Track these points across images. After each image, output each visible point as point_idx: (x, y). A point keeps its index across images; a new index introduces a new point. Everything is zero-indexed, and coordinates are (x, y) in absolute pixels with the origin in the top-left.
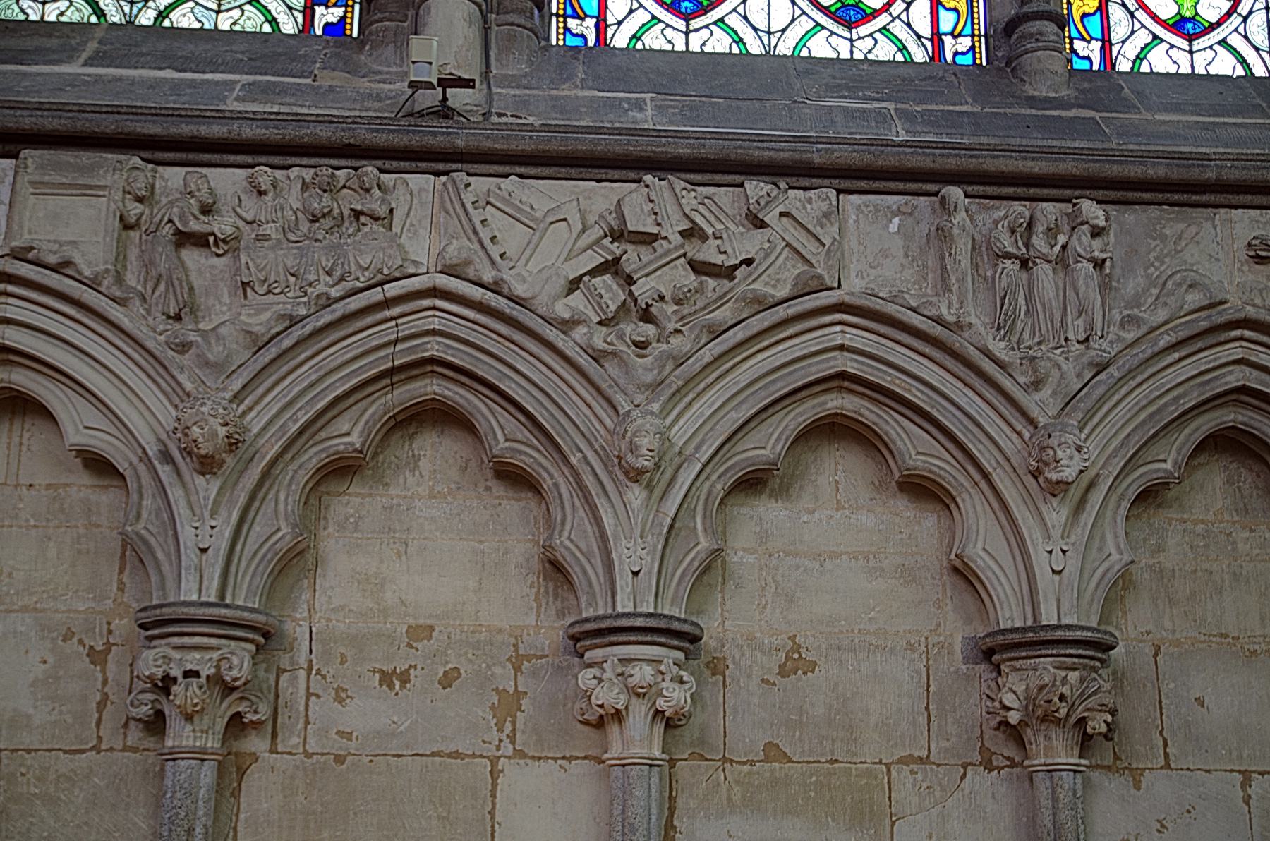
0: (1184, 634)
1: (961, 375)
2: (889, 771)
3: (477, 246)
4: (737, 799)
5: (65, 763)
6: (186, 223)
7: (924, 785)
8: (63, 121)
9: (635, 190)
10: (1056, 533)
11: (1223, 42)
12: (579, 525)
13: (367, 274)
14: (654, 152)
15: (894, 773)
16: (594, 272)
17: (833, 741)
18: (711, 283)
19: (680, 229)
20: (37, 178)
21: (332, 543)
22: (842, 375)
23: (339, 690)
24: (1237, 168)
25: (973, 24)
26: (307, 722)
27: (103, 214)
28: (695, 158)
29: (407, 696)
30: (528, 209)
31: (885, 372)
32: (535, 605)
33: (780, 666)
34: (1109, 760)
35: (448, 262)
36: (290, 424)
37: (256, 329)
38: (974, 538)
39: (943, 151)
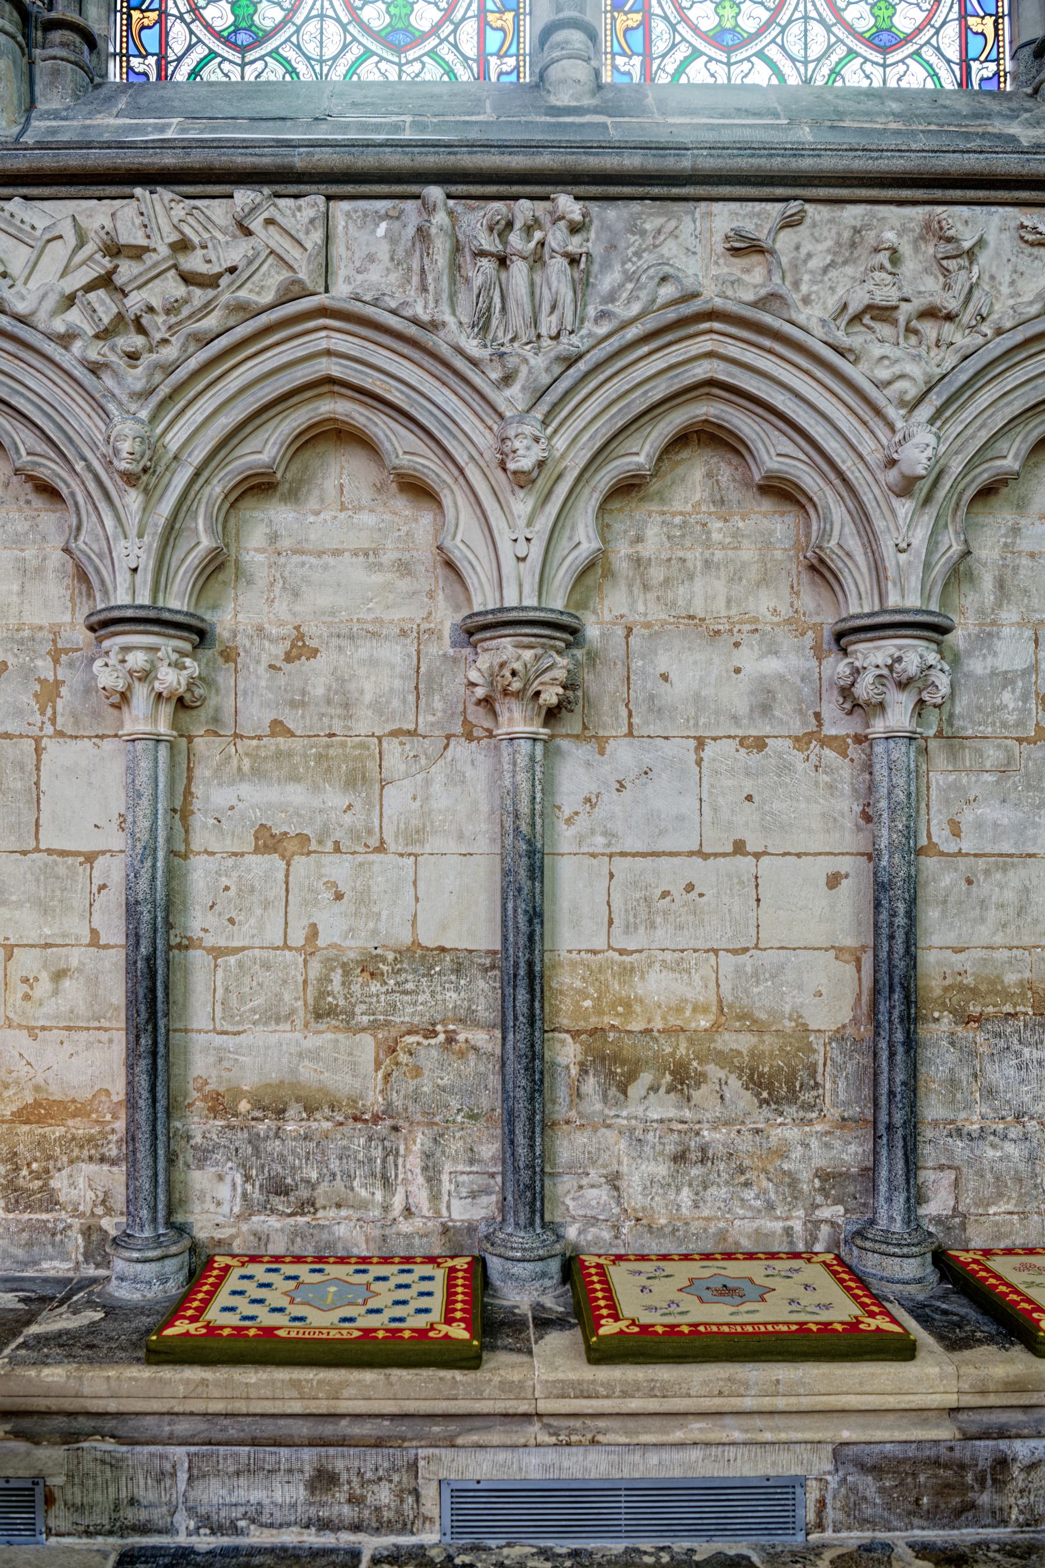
1: (437, 373)
2: (380, 742)
7: (411, 754)
10: (522, 523)
11: (760, 54)
14: (141, 164)
15: (385, 745)
16: (89, 288)
18: (197, 292)
19: (170, 240)
22: (330, 380)
25: (518, 43)
28: (182, 169)
30: (29, 229)
31: (367, 374)
32: (69, 605)
34: (577, 729)
38: (452, 530)
39: (423, 149)
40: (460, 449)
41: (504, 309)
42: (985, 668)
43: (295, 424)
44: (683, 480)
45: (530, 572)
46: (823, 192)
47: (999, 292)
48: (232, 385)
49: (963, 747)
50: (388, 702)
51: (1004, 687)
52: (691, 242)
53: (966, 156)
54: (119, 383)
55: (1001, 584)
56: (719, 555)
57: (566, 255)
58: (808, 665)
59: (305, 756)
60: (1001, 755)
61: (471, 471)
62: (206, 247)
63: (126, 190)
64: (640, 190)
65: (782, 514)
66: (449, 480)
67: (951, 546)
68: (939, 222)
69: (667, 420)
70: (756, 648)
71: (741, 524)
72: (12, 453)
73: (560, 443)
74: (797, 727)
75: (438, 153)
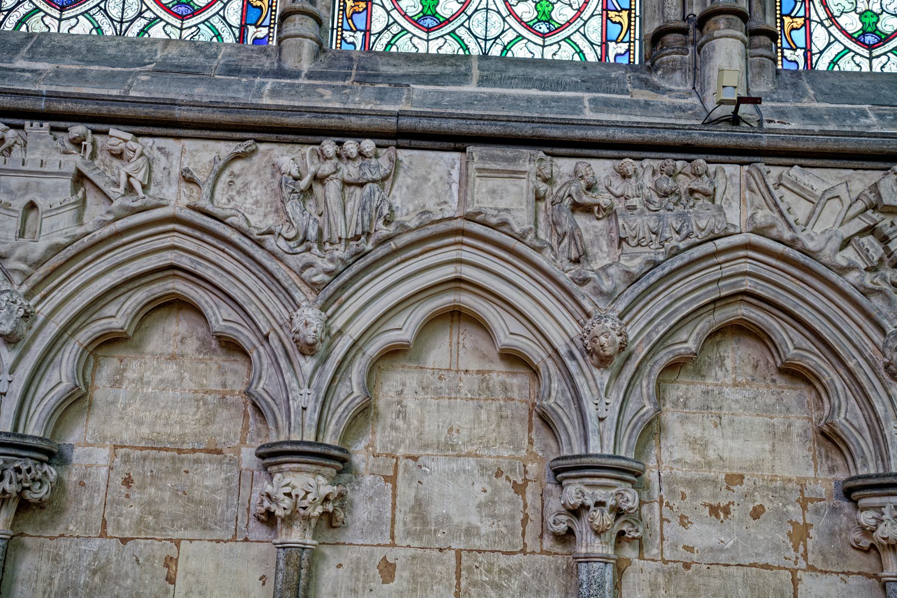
3: (777, 215)
5: (503, 561)
6: (581, 197)
8: (498, 128)
12: (852, 409)
13: (703, 233)
16: (862, 233)
20: (481, 165)
21: (670, 416)
23: (682, 517)
26: (662, 539)
27: (525, 190)
29: (729, 524)
30: (810, 189)
32: (812, 463)
35: (759, 226)
36: (654, 334)
37: (633, 270)
54: (890, 305)
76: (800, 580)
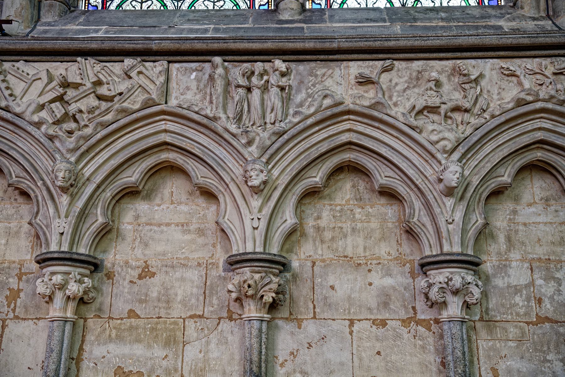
0: (327, 257)
1: (217, 140)
2: (184, 321)
4: (113, 335)
7: (200, 328)
9: (74, 65)
10: (256, 211)
12: (44, 213)
14: (81, 47)
15: (186, 323)
17: (160, 308)
19: (93, 80)
22: (166, 143)
24: (347, 41)
28: (100, 49)
30: (26, 75)
31: (183, 141)
32: (31, 250)
33: (139, 275)
34: (287, 315)
38: (223, 214)
40: (227, 175)
41: (249, 111)
42: (504, 283)
43: (148, 164)
44: (341, 188)
45: (259, 235)
46: (402, 56)
47: (492, 98)
48: (118, 146)
49: (496, 327)
50: (190, 300)
51: (516, 294)
52: (339, 79)
53: (470, 37)
54: (62, 145)
55: (509, 239)
56: (359, 225)
57: (278, 86)
58: (407, 281)
59: (145, 328)
60: (517, 331)
61: (232, 186)
62: (109, 84)
63: (74, 58)
64: (314, 57)
65: (391, 205)
66: (223, 190)
67: (477, 221)
68: (459, 67)
69: (330, 161)
70: (380, 272)
71: (370, 210)
72: (8, 176)
73: (276, 172)
74: (403, 315)
75: (219, 43)
76: (7, 326)
